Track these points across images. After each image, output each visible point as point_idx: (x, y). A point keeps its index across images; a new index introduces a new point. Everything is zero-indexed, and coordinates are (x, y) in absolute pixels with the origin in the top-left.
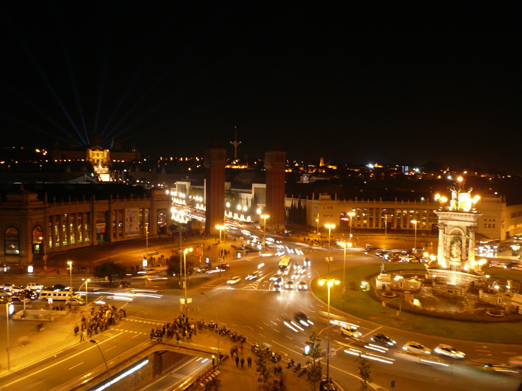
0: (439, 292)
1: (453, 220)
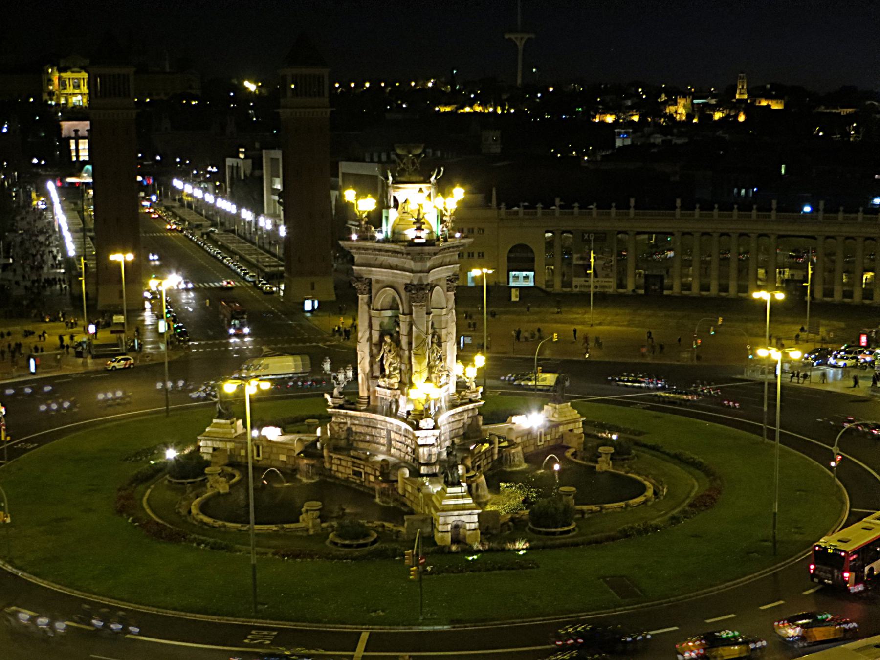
0: (340, 475)
1: (381, 266)
